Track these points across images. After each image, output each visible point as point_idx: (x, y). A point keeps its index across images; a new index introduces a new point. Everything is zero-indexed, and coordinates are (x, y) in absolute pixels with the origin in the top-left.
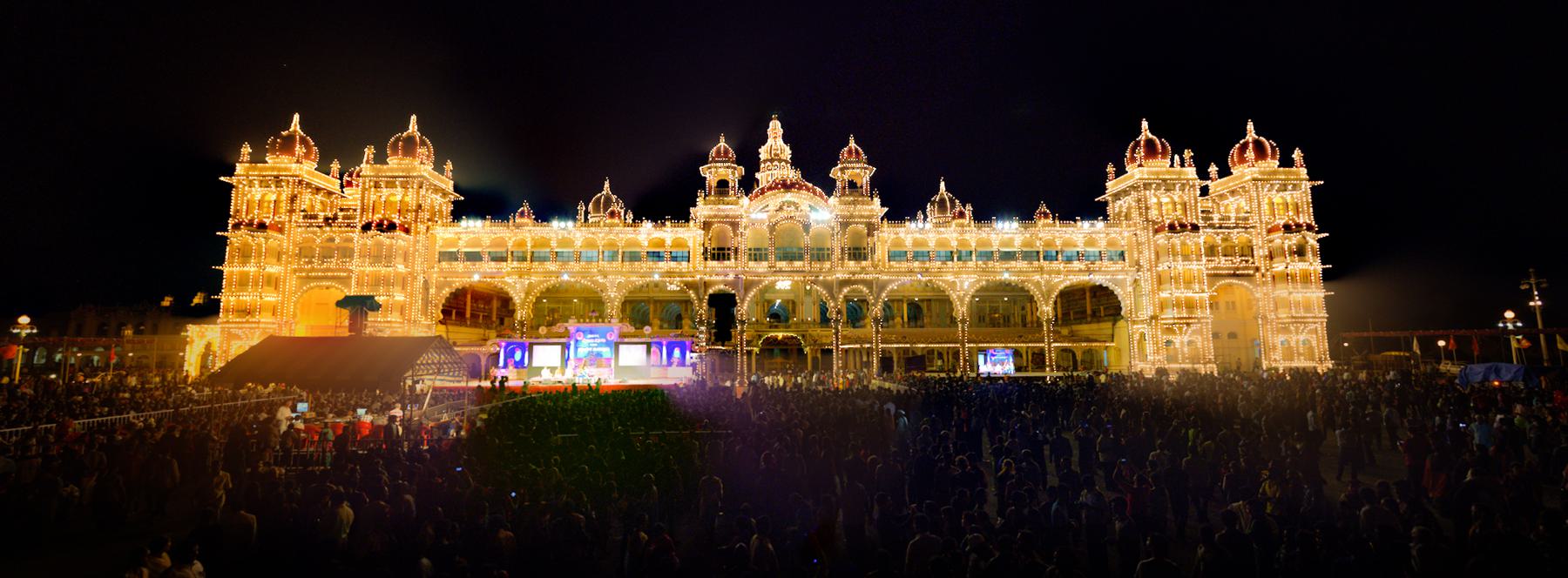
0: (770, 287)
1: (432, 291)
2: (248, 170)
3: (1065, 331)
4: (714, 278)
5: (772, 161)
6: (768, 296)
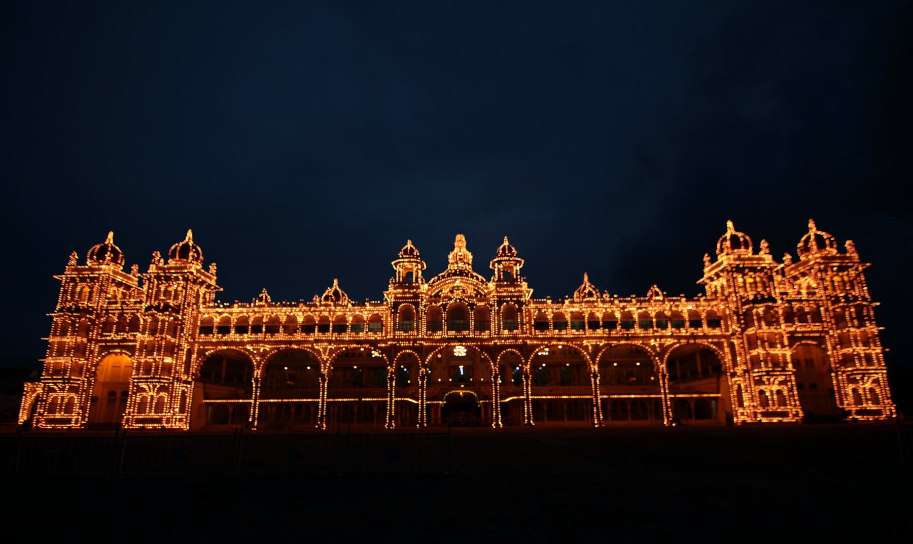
0: (449, 351)
3: (682, 386)
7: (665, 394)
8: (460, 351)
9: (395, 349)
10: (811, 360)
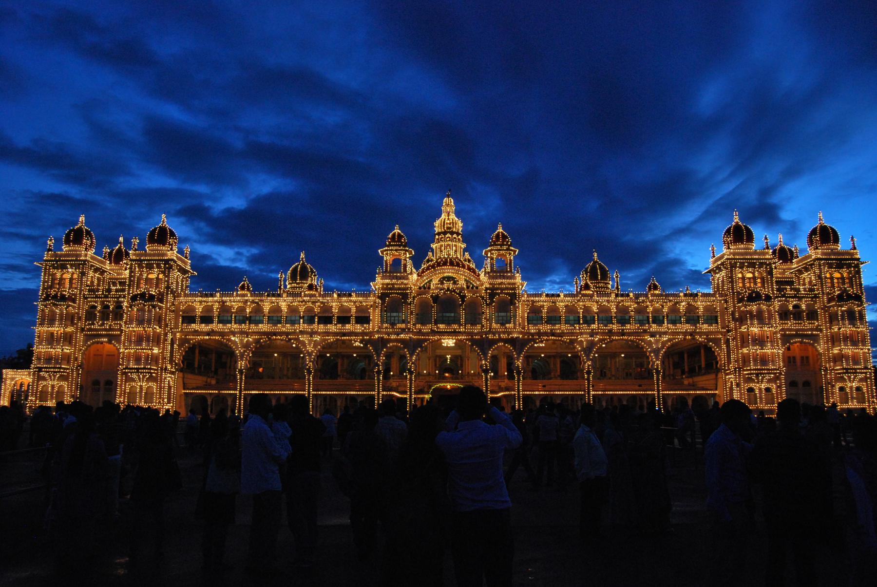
5: (445, 233)
6: (438, 352)
7: (658, 391)
8: (449, 342)
9: (383, 342)
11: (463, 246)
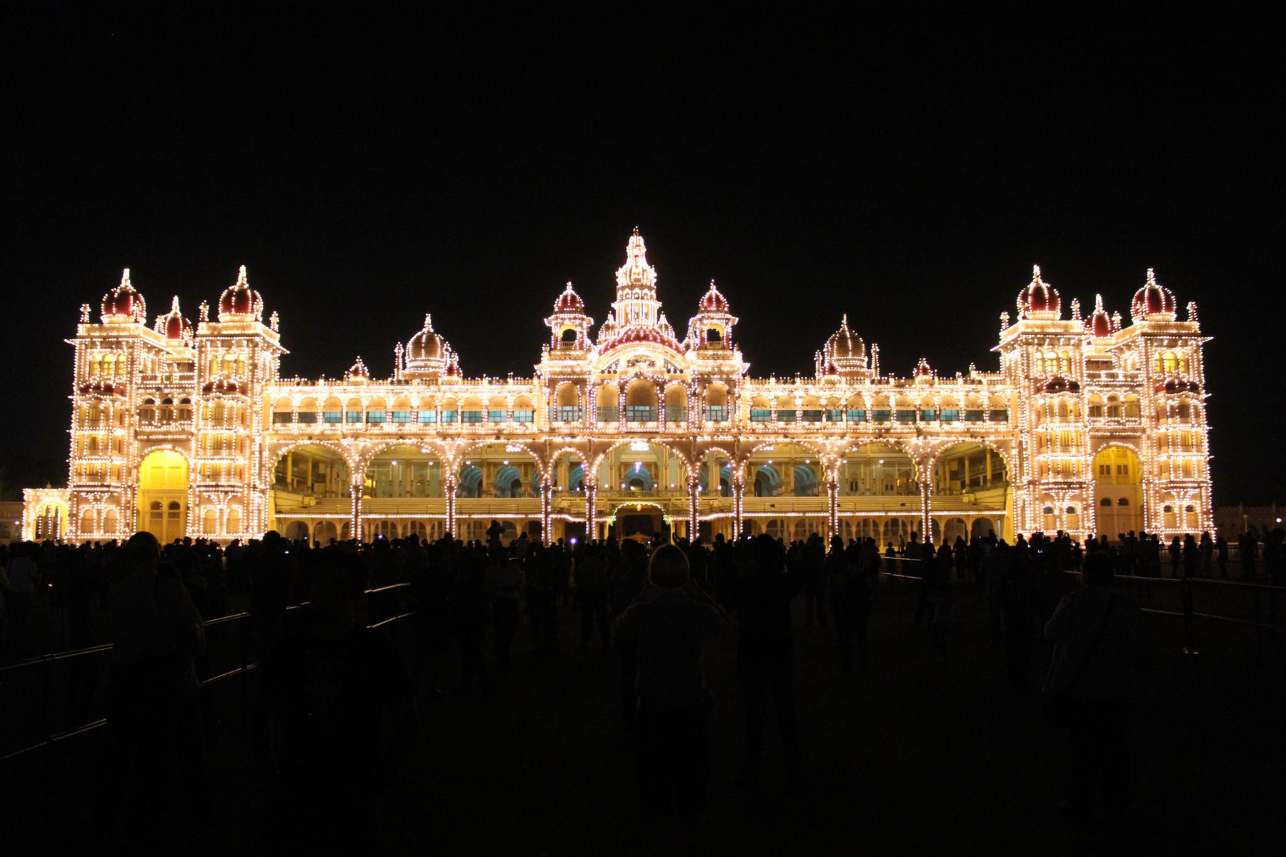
0: (624, 448)
1: (266, 454)
2: (89, 330)
4: (558, 440)
5: (632, 287)
7: (927, 512)
10: (1126, 467)
11: (659, 304)
